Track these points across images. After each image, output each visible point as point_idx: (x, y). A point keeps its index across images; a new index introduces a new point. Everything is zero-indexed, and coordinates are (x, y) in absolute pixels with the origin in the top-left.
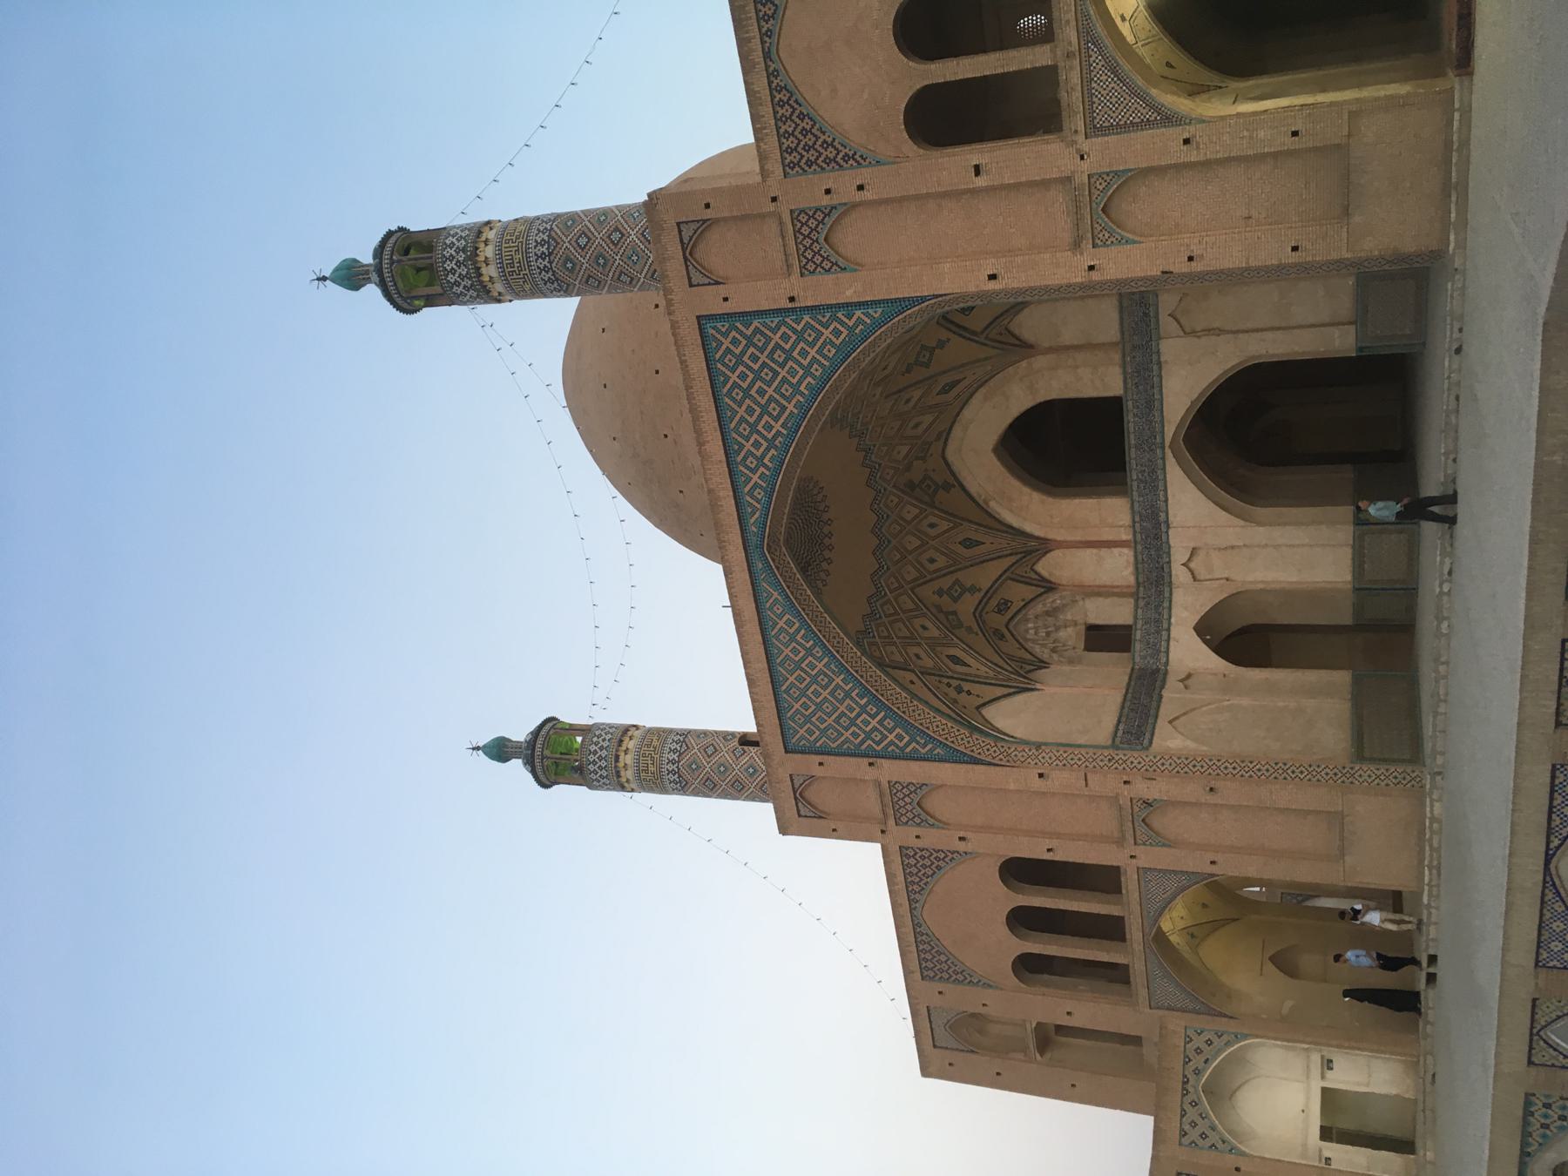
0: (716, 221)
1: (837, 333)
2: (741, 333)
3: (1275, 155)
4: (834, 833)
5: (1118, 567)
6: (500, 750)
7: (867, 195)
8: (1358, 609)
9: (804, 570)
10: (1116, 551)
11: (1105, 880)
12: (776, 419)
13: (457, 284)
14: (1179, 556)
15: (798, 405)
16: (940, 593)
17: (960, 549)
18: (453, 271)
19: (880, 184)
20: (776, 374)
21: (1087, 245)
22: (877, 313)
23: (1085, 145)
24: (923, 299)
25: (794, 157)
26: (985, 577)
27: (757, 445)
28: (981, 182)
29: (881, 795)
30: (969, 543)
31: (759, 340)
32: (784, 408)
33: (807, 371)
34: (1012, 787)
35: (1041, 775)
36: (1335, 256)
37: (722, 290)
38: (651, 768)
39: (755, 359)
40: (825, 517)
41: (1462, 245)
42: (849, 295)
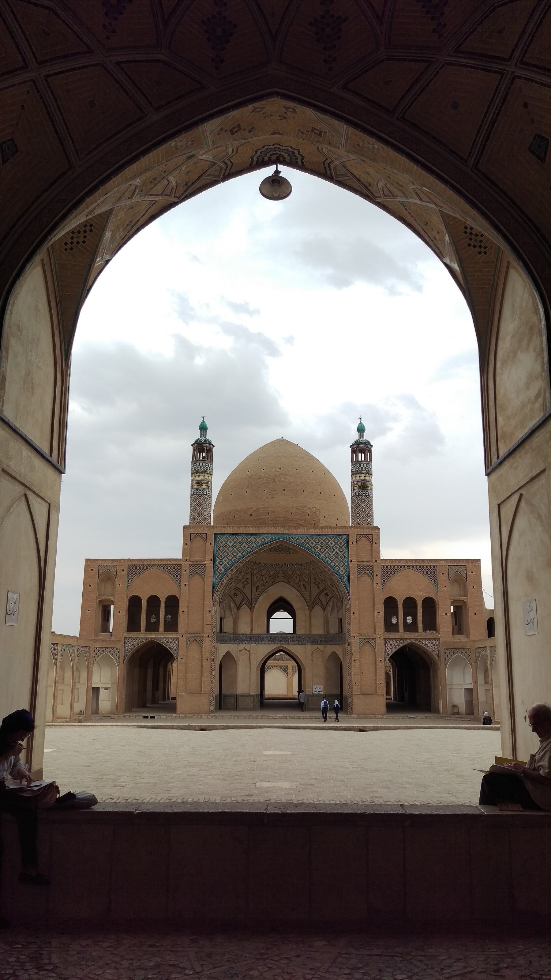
0: (372, 544)
1: (342, 571)
2: (343, 545)
3: (376, 680)
4: (185, 544)
5: (244, 629)
6: (203, 429)
7: (375, 584)
8: (227, 695)
9: (272, 548)
10: (250, 629)
11: (172, 626)
12: (319, 550)
13: (360, 466)
14: (248, 647)
15: (323, 557)
16: (247, 579)
17: (257, 585)
18: (364, 466)
19: (378, 588)
20: (332, 553)
21: (360, 637)
22: (347, 582)
23: (382, 638)
24: (349, 595)
25: (385, 568)
26: (247, 591)
27: (312, 543)
28: (376, 613)
29: (200, 562)
30: (258, 587)
31: (341, 550)
32: (322, 553)
33: (332, 561)
34: (206, 603)
35: (210, 611)
36: (353, 692)
37: (355, 543)
38: (204, 485)
39: (336, 548)
40: (281, 553)
41: (354, 718)
42: (352, 577)
